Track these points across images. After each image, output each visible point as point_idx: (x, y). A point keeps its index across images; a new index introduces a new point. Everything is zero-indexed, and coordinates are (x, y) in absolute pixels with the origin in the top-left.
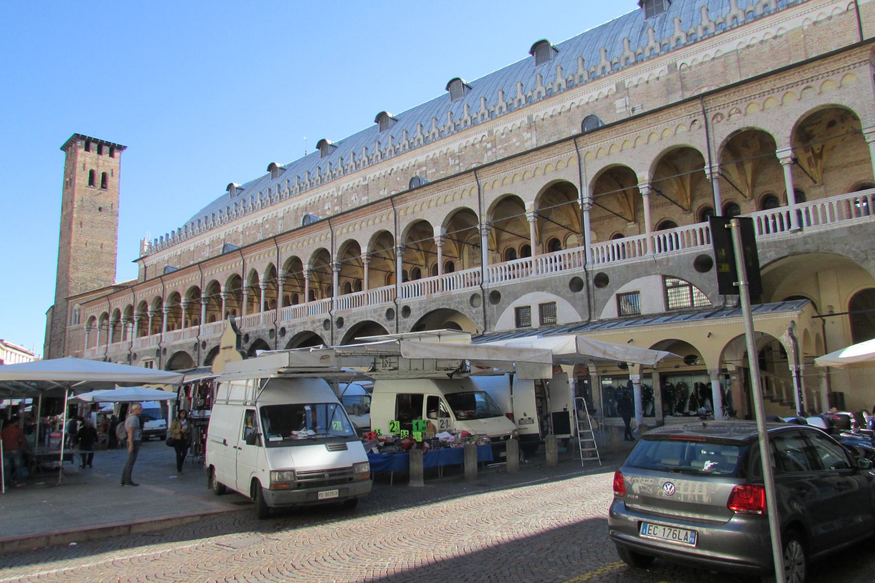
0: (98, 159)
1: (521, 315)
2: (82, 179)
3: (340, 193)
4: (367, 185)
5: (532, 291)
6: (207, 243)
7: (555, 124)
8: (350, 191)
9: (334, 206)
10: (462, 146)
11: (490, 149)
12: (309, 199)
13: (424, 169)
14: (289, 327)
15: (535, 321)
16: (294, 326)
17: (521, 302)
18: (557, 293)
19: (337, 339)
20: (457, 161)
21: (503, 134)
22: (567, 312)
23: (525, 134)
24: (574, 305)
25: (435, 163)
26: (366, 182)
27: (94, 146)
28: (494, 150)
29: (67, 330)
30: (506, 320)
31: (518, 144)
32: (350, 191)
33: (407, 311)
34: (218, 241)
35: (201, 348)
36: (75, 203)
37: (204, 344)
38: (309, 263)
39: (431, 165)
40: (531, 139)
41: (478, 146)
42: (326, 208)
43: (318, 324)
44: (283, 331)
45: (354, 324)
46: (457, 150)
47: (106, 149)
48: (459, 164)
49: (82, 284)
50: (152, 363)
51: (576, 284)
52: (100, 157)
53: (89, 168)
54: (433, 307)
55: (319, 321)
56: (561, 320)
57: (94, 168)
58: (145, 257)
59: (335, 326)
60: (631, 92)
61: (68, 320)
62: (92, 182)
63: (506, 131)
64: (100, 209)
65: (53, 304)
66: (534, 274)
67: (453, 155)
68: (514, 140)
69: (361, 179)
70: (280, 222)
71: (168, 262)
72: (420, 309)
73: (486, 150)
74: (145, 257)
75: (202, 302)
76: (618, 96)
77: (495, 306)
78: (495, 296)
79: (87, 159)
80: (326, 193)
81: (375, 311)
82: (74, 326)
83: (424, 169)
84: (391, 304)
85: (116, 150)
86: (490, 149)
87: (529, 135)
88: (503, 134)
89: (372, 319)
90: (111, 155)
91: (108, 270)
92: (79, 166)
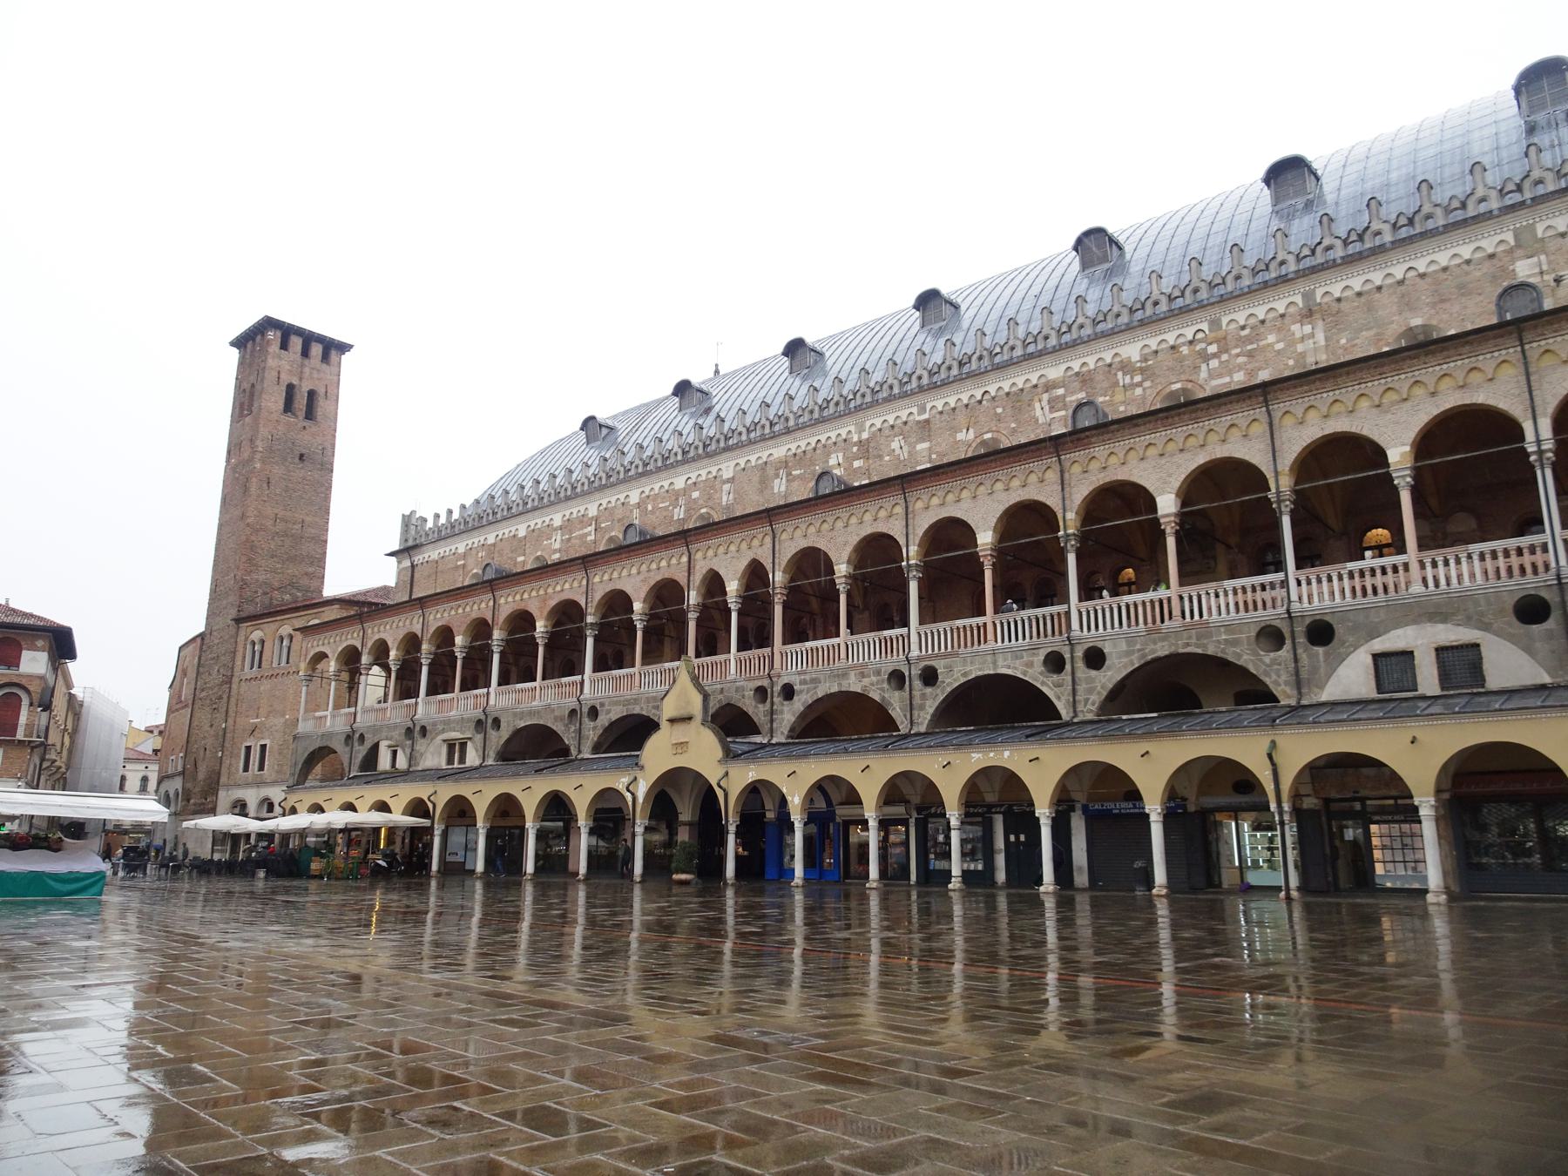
0: (302, 365)
1: (1393, 669)
2: (273, 400)
3: (865, 436)
4: (927, 421)
5: (1415, 622)
6: (558, 522)
7: (1370, 308)
8: (887, 432)
9: (849, 459)
10: (1146, 351)
11: (1215, 356)
12: (793, 446)
13: (1061, 391)
14: (803, 682)
15: (1428, 679)
16: (815, 681)
17: (1381, 644)
18: (1486, 627)
19: (922, 707)
20: (1138, 379)
21: (1243, 328)
22: (1508, 662)
23: (1296, 328)
24: (1529, 650)
25: (1084, 382)
26: (926, 416)
27: (296, 343)
28: (1225, 357)
29: (235, 680)
30: (1352, 676)
31: (1280, 346)
32: (887, 432)
33: (1095, 658)
34: (583, 520)
35: (586, 720)
36: (259, 443)
37: (594, 713)
38: (849, 562)
39: (1077, 385)
40: (1312, 335)
41: (1185, 350)
42: (833, 462)
43: (874, 679)
44: (788, 692)
45: (963, 680)
46: (1136, 357)
47: (317, 350)
48: (1139, 384)
49: (265, 593)
50: (463, 746)
51: (1531, 610)
52: (306, 362)
53: (286, 379)
54: (1162, 650)
55: (878, 673)
56: (1496, 678)
57: (295, 381)
58: (415, 547)
59: (917, 684)
60: (1552, 246)
61: (238, 663)
62: (288, 406)
63: (1252, 321)
64: (301, 457)
65: (200, 628)
66: (1417, 588)
67: (1126, 367)
68: (1271, 338)
69: (915, 410)
70: (726, 487)
71: (464, 556)
72: (1128, 653)
73: (1206, 357)
74: (415, 547)
75: (588, 632)
76: (1519, 252)
77: (1320, 650)
78: (1321, 633)
79: (281, 363)
80: (833, 435)
81: (1016, 654)
82: (248, 673)
83: (1061, 391)
84: (1056, 643)
85: (333, 353)
86: (1215, 356)
87: (1308, 329)
88: (1243, 328)
89: (1009, 672)
90: (325, 357)
91: (311, 570)
92: (270, 376)
